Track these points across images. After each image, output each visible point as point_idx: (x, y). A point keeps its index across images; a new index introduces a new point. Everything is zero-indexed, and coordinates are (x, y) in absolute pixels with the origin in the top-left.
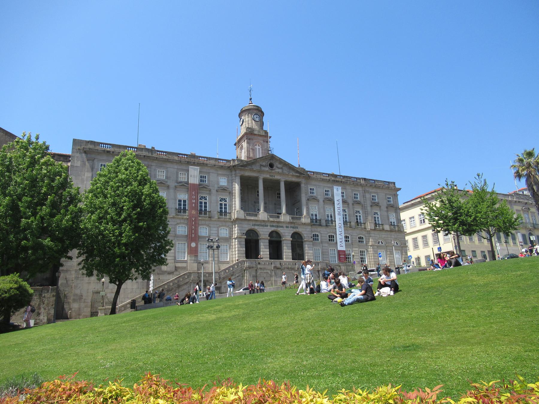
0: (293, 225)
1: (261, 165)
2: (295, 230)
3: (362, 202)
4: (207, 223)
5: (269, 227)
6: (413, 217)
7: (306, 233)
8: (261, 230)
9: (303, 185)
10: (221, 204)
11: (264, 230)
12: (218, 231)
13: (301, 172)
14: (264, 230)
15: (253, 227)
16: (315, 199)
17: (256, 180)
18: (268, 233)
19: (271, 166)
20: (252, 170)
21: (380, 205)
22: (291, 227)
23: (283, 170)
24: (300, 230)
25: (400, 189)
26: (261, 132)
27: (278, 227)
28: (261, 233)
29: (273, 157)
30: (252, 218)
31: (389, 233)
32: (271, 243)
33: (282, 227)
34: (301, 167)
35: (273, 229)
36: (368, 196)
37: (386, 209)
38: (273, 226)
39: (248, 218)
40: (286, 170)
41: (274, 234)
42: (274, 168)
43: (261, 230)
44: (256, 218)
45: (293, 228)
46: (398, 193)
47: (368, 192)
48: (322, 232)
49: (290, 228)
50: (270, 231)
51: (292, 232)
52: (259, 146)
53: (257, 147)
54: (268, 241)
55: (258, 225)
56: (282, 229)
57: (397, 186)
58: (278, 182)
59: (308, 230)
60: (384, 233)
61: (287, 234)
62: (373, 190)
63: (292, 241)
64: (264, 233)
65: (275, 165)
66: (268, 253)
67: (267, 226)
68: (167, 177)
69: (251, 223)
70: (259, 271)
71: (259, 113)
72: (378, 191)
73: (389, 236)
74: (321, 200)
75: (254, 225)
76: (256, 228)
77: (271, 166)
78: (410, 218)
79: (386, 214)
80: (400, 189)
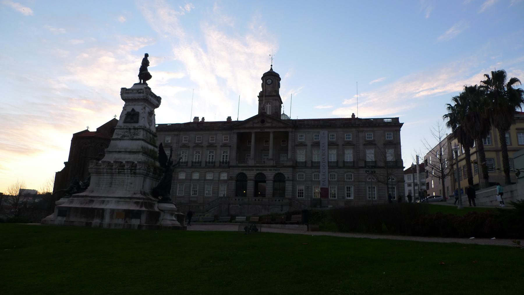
0: (275, 168)
2: (277, 172)
4: (212, 169)
7: (287, 173)
9: (290, 134)
10: (224, 156)
12: (219, 175)
16: (303, 145)
17: (250, 134)
20: (245, 128)
24: (282, 171)
25: (403, 124)
27: (262, 170)
28: (248, 176)
30: (243, 165)
33: (266, 170)
35: (258, 172)
36: (361, 135)
38: (258, 170)
39: (240, 165)
45: (276, 170)
47: (362, 131)
50: (256, 173)
51: (274, 174)
53: (268, 105)
55: (246, 170)
57: (401, 121)
62: (369, 129)
64: (251, 174)
67: (253, 170)
68: (189, 141)
70: (231, 206)
72: (375, 129)
76: (244, 172)
80: (403, 124)
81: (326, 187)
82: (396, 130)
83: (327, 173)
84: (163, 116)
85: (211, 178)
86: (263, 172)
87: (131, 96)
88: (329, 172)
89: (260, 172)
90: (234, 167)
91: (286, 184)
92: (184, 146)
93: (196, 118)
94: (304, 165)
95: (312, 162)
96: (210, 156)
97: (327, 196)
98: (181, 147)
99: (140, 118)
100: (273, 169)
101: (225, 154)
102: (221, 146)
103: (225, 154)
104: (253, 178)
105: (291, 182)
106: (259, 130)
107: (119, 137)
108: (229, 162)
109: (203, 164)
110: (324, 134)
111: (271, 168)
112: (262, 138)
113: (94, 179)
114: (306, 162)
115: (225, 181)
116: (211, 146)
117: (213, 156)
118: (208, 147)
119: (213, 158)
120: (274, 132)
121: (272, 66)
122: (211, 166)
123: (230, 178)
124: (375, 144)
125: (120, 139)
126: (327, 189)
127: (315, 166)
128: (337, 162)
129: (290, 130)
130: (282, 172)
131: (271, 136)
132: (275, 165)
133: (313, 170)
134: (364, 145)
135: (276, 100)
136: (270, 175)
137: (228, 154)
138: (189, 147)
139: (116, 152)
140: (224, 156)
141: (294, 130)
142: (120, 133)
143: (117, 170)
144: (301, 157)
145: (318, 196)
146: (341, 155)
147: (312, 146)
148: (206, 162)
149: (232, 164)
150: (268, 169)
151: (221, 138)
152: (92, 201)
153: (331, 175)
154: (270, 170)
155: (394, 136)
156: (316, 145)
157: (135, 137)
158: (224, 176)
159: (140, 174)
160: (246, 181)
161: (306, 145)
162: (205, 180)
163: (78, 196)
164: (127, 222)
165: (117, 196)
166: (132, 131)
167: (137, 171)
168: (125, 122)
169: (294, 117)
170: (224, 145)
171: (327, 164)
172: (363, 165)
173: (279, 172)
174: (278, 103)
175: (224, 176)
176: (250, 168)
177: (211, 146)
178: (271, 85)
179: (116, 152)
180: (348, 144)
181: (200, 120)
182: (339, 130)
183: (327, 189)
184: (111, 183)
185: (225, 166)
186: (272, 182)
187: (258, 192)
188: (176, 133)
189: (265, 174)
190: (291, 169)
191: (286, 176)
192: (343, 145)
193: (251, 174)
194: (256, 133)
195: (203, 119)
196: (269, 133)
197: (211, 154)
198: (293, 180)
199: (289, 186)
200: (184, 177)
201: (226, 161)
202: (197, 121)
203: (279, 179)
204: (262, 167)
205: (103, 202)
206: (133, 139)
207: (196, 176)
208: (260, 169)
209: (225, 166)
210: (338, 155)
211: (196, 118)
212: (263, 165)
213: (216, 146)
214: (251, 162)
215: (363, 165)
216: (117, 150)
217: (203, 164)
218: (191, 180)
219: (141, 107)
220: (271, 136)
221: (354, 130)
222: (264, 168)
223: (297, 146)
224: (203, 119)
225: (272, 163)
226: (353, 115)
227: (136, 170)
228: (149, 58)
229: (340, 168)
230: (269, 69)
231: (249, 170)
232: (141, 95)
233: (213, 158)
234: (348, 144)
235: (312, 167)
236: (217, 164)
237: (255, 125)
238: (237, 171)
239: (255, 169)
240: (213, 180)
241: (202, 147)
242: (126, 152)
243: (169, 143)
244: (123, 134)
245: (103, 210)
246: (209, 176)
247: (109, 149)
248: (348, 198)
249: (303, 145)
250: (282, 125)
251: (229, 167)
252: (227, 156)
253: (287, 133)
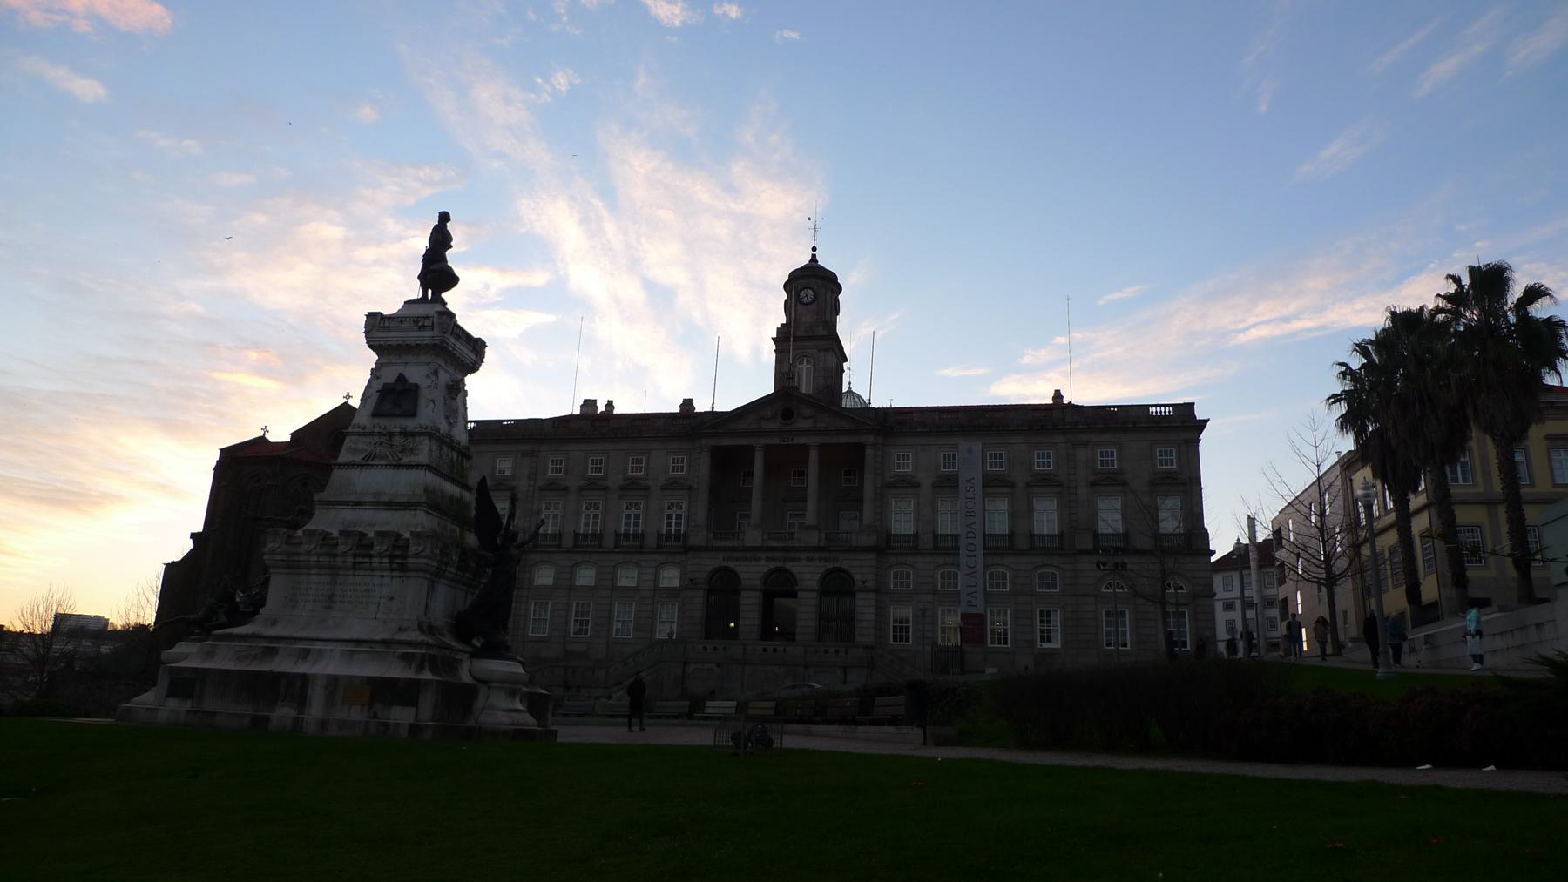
2: (830, 566)
7: (861, 569)
9: (869, 452)
10: (670, 516)
16: (908, 484)
17: (750, 450)
24: (845, 562)
28: (742, 576)
30: (727, 543)
33: (799, 560)
35: (773, 565)
36: (1082, 455)
38: (773, 559)
39: (719, 543)
44: (736, 544)
45: (826, 560)
50: (766, 569)
53: (805, 366)
55: (737, 559)
57: (1199, 415)
62: (1107, 437)
64: (752, 573)
68: (566, 472)
76: (732, 564)
81: (980, 609)
82: (1186, 441)
83: (980, 566)
84: (490, 396)
85: (633, 584)
86: (788, 565)
87: (395, 336)
88: (986, 567)
90: (699, 549)
91: (859, 603)
92: (554, 487)
93: (589, 404)
94: (912, 545)
95: (935, 536)
96: (628, 516)
97: (981, 639)
98: (541, 489)
99: (422, 402)
100: (817, 555)
101: (674, 512)
102: (663, 488)
103: (674, 512)
105: (873, 596)
106: (776, 441)
107: (358, 458)
108: (685, 535)
109: (609, 542)
110: (970, 451)
112: (786, 462)
113: (278, 585)
114: (916, 536)
115: (673, 593)
116: (633, 487)
117: (637, 517)
118: (622, 488)
119: (637, 524)
120: (821, 447)
121: (814, 249)
122: (632, 546)
123: (689, 584)
124: (1124, 484)
125: (361, 466)
126: (982, 617)
127: (946, 547)
128: (1012, 535)
130: (845, 565)
131: (814, 456)
134: (1093, 484)
135: (826, 350)
136: (808, 574)
137: (683, 512)
138: (566, 489)
139: (347, 503)
140: (670, 516)
141: (880, 440)
142: (360, 446)
143: (350, 559)
144: (902, 522)
145: (955, 640)
147: (934, 486)
148: (617, 535)
149: (695, 540)
150: (803, 555)
151: (663, 462)
152: (271, 652)
153: (991, 575)
154: (808, 559)
155: (1179, 459)
156: (948, 483)
157: (405, 460)
158: (671, 578)
159: (417, 570)
160: (738, 593)
161: (917, 486)
162: (614, 588)
163: (231, 637)
164: (375, 716)
165: (347, 637)
166: (397, 440)
167: (410, 560)
168: (374, 415)
169: (882, 396)
170: (672, 485)
171: (979, 541)
172: (1090, 546)
173: (837, 565)
174: (832, 360)
175: (671, 578)
177: (633, 487)
179: (347, 503)
180: (1045, 482)
181: (601, 408)
183: (982, 617)
184: (331, 597)
185: (675, 546)
186: (814, 595)
187: (774, 626)
188: (528, 448)
190: (873, 556)
191: (857, 577)
192: (1028, 485)
193: (752, 573)
194: (767, 448)
195: (610, 404)
196: (805, 448)
197: (633, 511)
198: (877, 591)
199: (865, 607)
200: (548, 581)
201: (678, 531)
202: (590, 411)
203: (837, 585)
204: (784, 549)
205: (305, 654)
206: (398, 466)
207: (586, 577)
208: (778, 555)
209: (675, 546)
210: (1013, 515)
211: (589, 404)
212: (790, 544)
213: (647, 488)
214: (752, 537)
215: (1090, 546)
216: (352, 498)
217: (609, 542)
218: (572, 588)
219: (424, 370)
220: (814, 456)
221: (1060, 439)
222: (792, 555)
223: (890, 486)
224: (610, 404)
225: (814, 539)
226: (1058, 395)
227: (405, 557)
228: (449, 226)
230: (806, 260)
232: (427, 334)
233: (637, 524)
234: (1045, 482)
236: (651, 541)
237: (766, 425)
238: (710, 563)
240: (636, 589)
241: (606, 489)
242: (378, 503)
243: (507, 478)
244: (369, 448)
245: (305, 678)
246: (627, 578)
247: (325, 495)
248: (1046, 645)
249: (908, 484)
251: (687, 549)
252: (679, 517)
253: (861, 448)
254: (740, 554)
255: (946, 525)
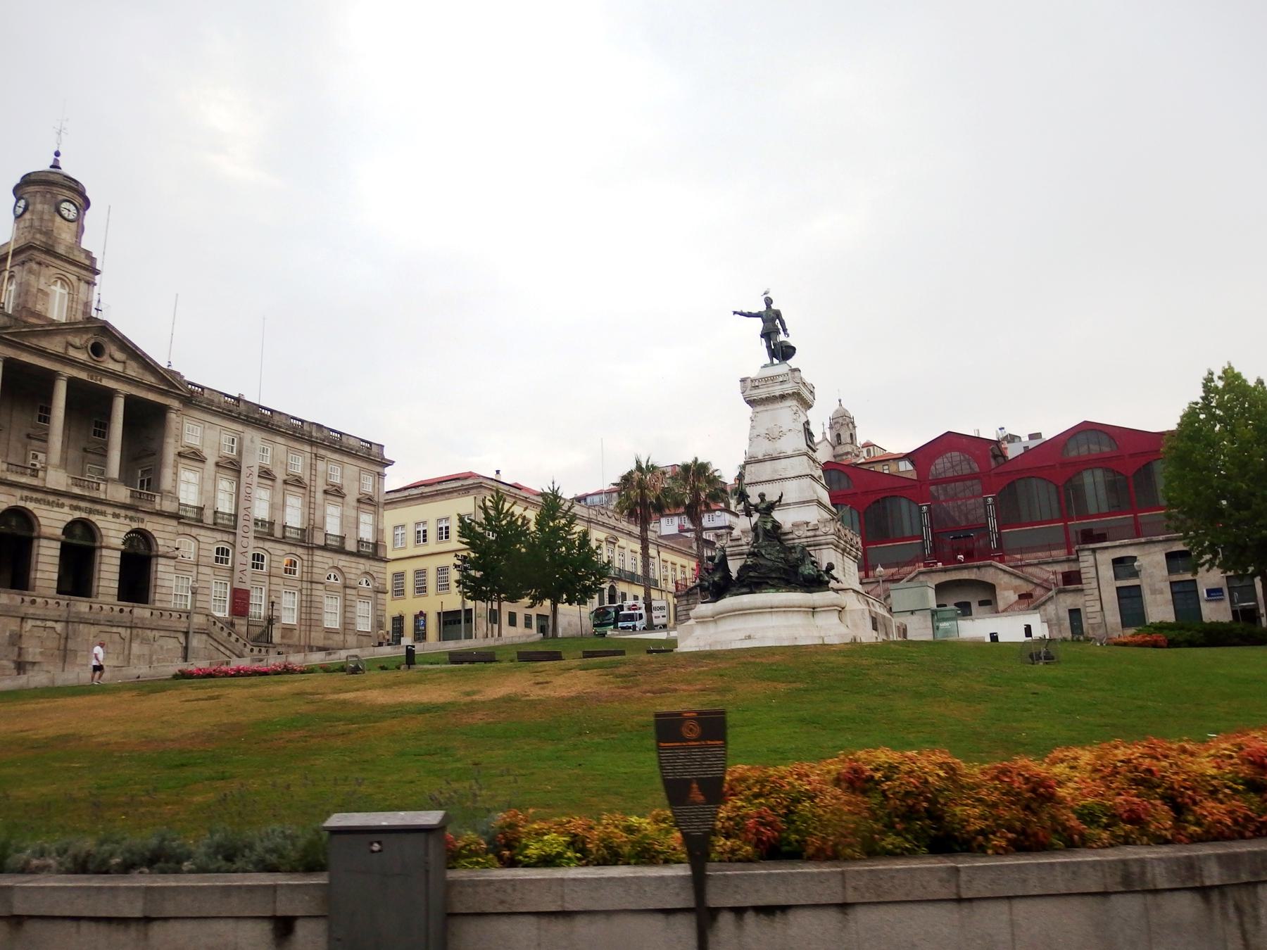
0: (131, 513)
1: (69, 344)
2: (135, 525)
3: (307, 481)
5: (66, 509)
6: (403, 526)
7: (163, 534)
8: (44, 514)
9: (172, 416)
11: (52, 515)
13: (168, 381)
14: (52, 515)
15: (22, 504)
16: (195, 456)
17: (51, 377)
18: (63, 525)
19: (97, 350)
20: (42, 353)
21: (344, 491)
22: (126, 517)
23: (125, 368)
24: (150, 525)
26: (76, 253)
27: (91, 511)
28: (42, 521)
29: (105, 329)
30: (23, 480)
31: (353, 559)
32: (66, 550)
33: (103, 514)
34: (174, 368)
35: (77, 514)
36: (321, 465)
37: (355, 504)
40: (133, 370)
41: (78, 531)
42: (105, 357)
43: (44, 514)
44: (35, 482)
45: (132, 519)
46: (387, 470)
47: (323, 458)
48: (200, 538)
49: (122, 520)
50: (70, 519)
52: (62, 286)
54: (58, 545)
55: (37, 501)
56: (101, 517)
57: (388, 455)
58: (110, 395)
59: (170, 529)
60: (343, 557)
61: (112, 533)
62: (336, 456)
63: (124, 554)
65: (107, 351)
66: (55, 576)
67: (62, 506)
69: (19, 493)
71: (79, 201)
72: (346, 459)
73: (354, 565)
74: (211, 460)
75: (26, 499)
76: (30, 506)
77: (97, 350)
78: (396, 527)
79: (353, 513)
86: (93, 518)
89: (84, 515)
100: (123, 512)
104: (59, 532)
106: (83, 376)
111: (117, 511)
114: (200, 509)
121: (57, 154)
124: (343, 496)
126: (247, 592)
129: (175, 404)
130: (148, 526)
132: (128, 501)
133: (219, 536)
134: (326, 492)
136: (113, 532)
146: (278, 506)
150: (110, 510)
154: (116, 516)
156: (233, 466)
173: (142, 526)
176: (51, 498)
178: (73, 226)
180: (296, 482)
182: (279, 439)
183: (247, 592)
189: (99, 524)
194: (72, 383)
208: (83, 504)
212: (94, 494)
214: (57, 479)
221: (308, 448)
222: (98, 507)
229: (276, 541)
231: (48, 503)
234: (296, 482)
235: (216, 527)
237: (72, 353)
239: (67, 501)
250: (150, 379)
253: (162, 410)
254: (39, 496)
255: (225, 505)
